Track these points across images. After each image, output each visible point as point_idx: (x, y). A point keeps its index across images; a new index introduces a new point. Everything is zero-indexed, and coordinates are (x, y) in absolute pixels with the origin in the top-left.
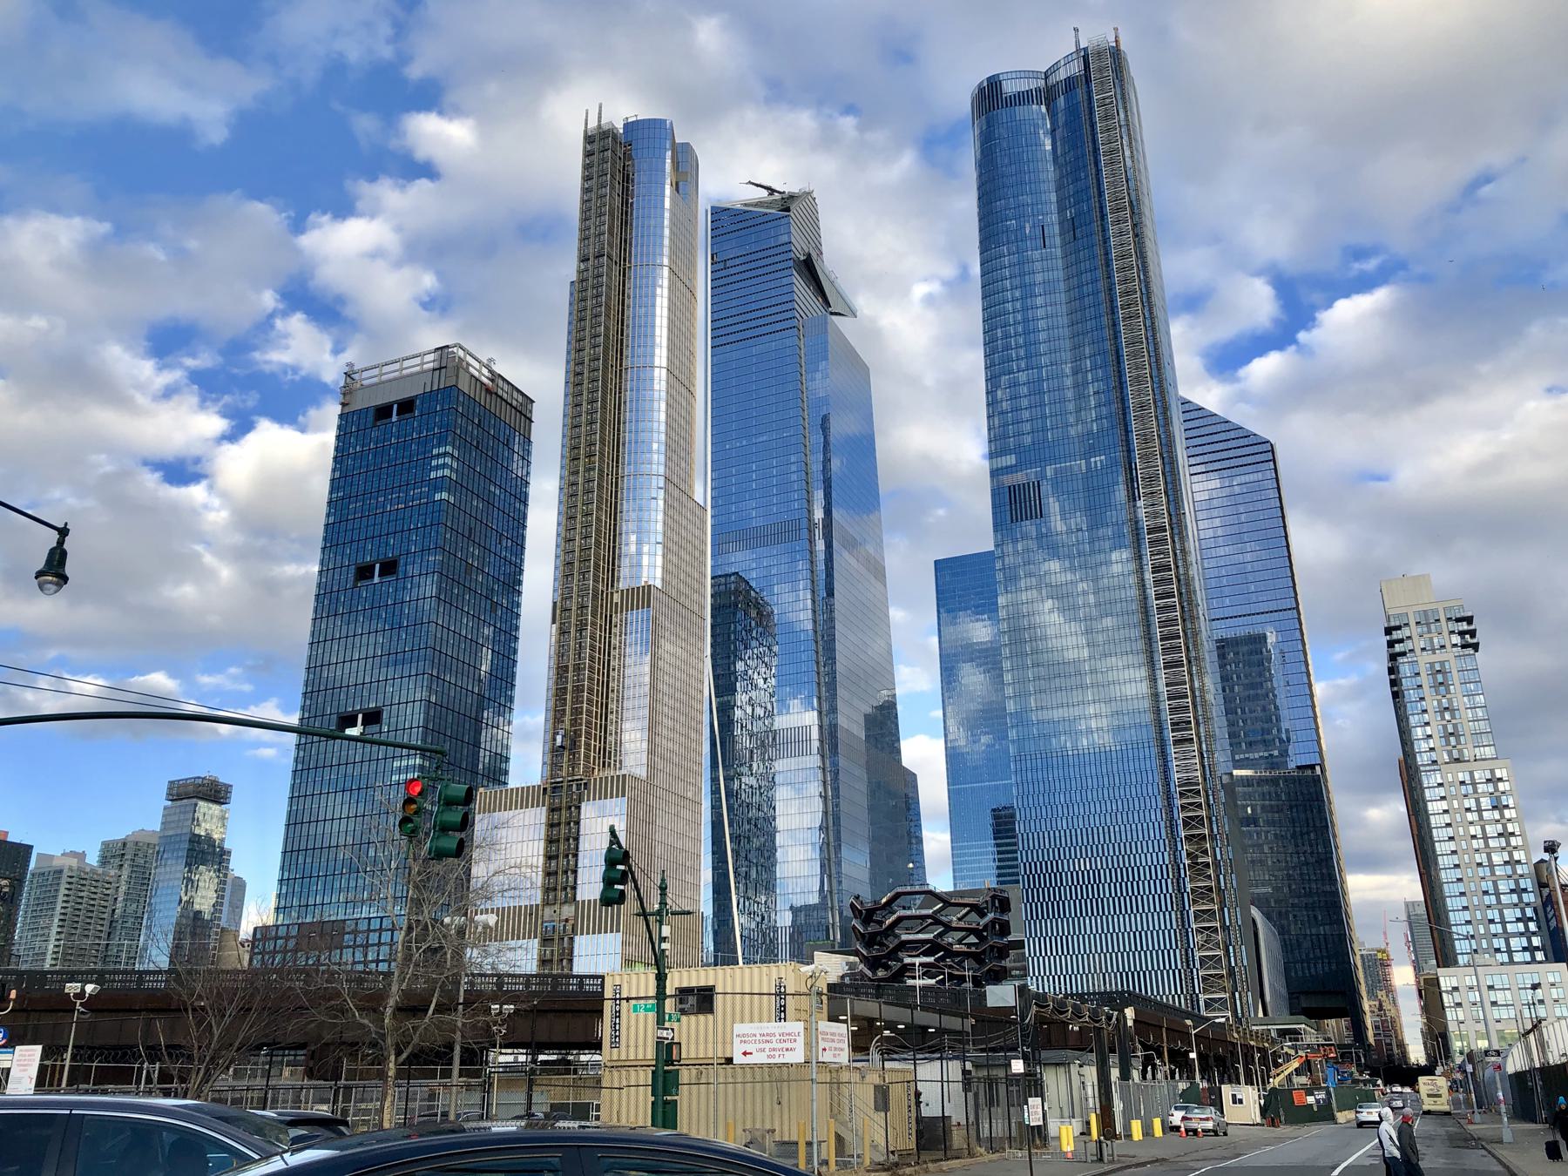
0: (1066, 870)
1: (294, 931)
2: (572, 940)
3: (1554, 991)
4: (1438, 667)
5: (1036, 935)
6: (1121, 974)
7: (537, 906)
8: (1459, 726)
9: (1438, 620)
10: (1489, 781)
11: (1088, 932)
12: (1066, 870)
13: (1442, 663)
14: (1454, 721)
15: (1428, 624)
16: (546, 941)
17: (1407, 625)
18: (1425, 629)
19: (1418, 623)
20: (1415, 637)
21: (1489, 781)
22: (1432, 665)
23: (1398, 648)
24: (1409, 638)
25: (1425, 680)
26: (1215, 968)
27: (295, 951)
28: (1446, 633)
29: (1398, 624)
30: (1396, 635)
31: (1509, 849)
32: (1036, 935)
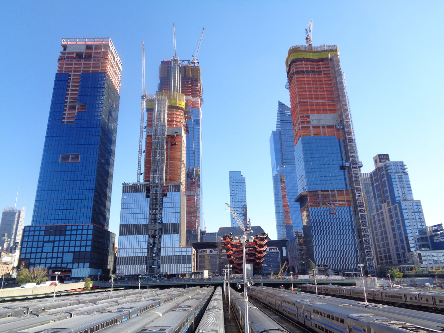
0: (324, 222)
1: (43, 228)
2: (160, 237)
3: (428, 257)
4: (400, 177)
5: (316, 239)
6: (334, 251)
7: (147, 224)
8: (405, 192)
9: (398, 165)
10: (416, 205)
11: (330, 239)
12: (324, 222)
13: (401, 176)
14: (404, 190)
15: (396, 166)
17: (391, 166)
18: (395, 167)
19: (393, 165)
20: (393, 169)
21: (416, 205)
22: (399, 176)
23: (389, 171)
24: (392, 169)
25: (397, 180)
26: (369, 250)
27: (44, 236)
28: (400, 169)
29: (389, 165)
30: (389, 168)
31: (421, 222)
32: (316, 239)
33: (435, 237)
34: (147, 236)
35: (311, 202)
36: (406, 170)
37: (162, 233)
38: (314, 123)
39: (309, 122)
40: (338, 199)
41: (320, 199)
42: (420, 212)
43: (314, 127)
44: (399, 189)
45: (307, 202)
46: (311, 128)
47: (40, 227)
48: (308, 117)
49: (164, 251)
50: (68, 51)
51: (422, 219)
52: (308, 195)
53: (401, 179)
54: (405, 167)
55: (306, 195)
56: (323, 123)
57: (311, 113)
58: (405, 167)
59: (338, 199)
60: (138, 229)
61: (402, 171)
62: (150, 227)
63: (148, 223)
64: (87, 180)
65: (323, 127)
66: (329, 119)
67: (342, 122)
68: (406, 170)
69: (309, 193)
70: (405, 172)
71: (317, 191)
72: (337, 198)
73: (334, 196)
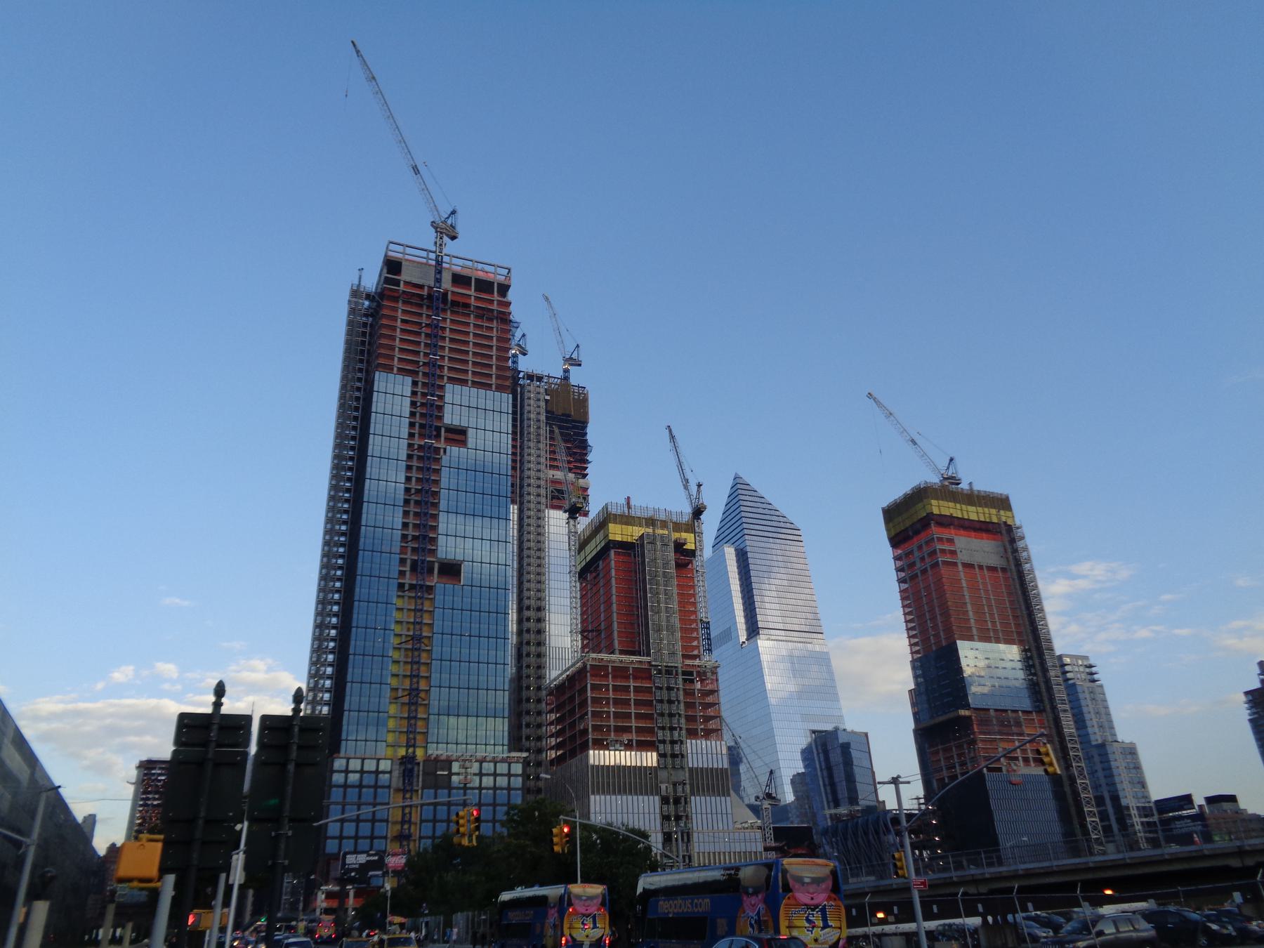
4: (1090, 690)
16: (665, 800)
25: (1088, 696)
33: (1177, 822)
34: (657, 798)
35: (981, 733)
36: (1096, 677)
37: (693, 794)
38: (963, 557)
39: (953, 553)
40: (1027, 731)
41: (996, 728)
42: (1138, 767)
43: (966, 565)
44: (1093, 716)
45: (974, 733)
46: (960, 567)
47: (378, 760)
48: (951, 541)
49: (701, 840)
50: (405, 276)
51: (1143, 784)
52: (973, 717)
53: (1092, 695)
54: (1094, 670)
55: (969, 717)
56: (978, 559)
57: (956, 535)
58: (1094, 670)
59: (1027, 731)
60: (635, 778)
61: (1089, 677)
62: (663, 775)
63: (655, 764)
64: (470, 636)
65: (981, 567)
66: (988, 552)
67: (1018, 564)
68: (1096, 677)
69: (976, 713)
70: (1094, 681)
71: (988, 710)
72: (1024, 727)
73: (1018, 724)
